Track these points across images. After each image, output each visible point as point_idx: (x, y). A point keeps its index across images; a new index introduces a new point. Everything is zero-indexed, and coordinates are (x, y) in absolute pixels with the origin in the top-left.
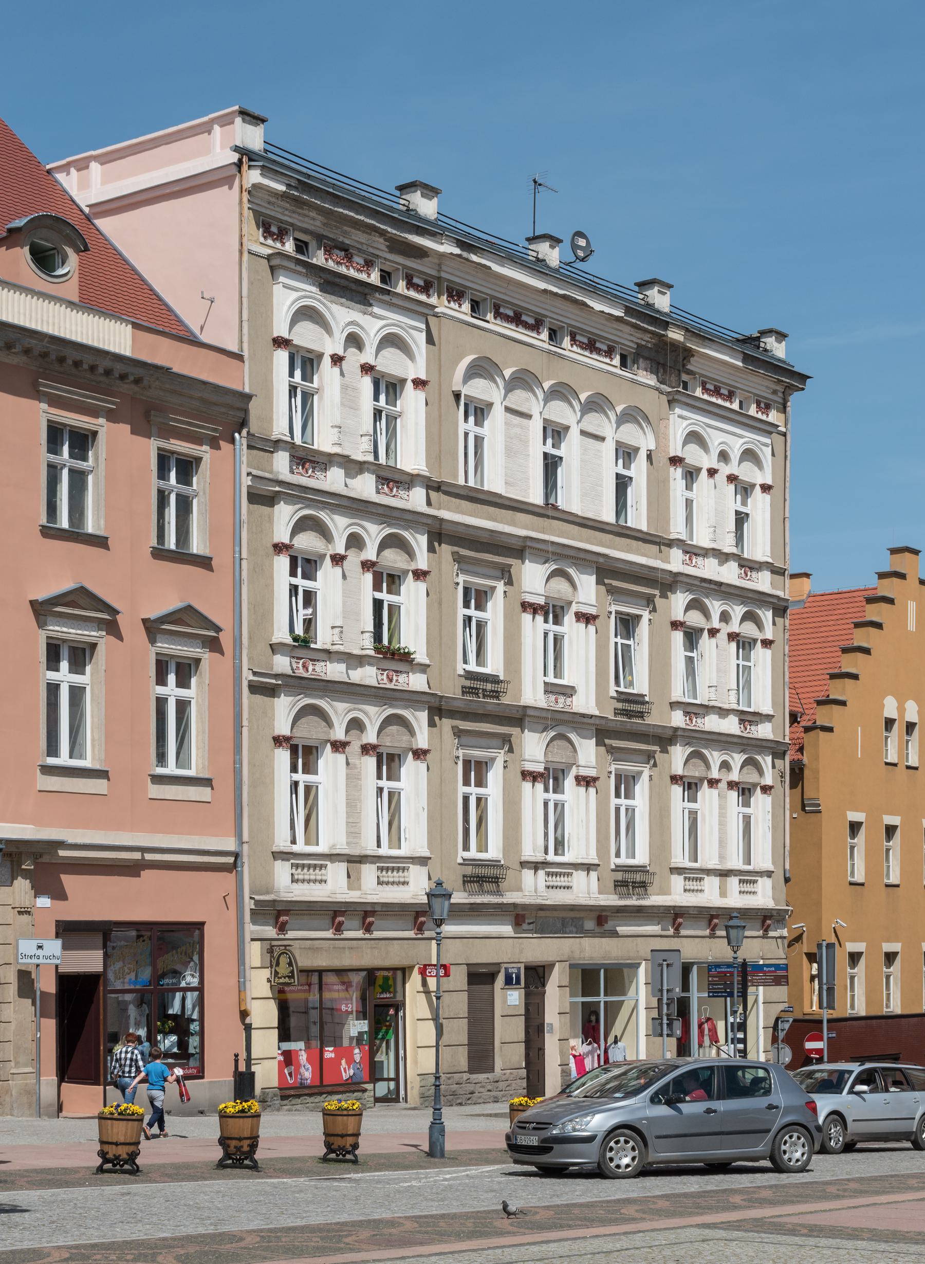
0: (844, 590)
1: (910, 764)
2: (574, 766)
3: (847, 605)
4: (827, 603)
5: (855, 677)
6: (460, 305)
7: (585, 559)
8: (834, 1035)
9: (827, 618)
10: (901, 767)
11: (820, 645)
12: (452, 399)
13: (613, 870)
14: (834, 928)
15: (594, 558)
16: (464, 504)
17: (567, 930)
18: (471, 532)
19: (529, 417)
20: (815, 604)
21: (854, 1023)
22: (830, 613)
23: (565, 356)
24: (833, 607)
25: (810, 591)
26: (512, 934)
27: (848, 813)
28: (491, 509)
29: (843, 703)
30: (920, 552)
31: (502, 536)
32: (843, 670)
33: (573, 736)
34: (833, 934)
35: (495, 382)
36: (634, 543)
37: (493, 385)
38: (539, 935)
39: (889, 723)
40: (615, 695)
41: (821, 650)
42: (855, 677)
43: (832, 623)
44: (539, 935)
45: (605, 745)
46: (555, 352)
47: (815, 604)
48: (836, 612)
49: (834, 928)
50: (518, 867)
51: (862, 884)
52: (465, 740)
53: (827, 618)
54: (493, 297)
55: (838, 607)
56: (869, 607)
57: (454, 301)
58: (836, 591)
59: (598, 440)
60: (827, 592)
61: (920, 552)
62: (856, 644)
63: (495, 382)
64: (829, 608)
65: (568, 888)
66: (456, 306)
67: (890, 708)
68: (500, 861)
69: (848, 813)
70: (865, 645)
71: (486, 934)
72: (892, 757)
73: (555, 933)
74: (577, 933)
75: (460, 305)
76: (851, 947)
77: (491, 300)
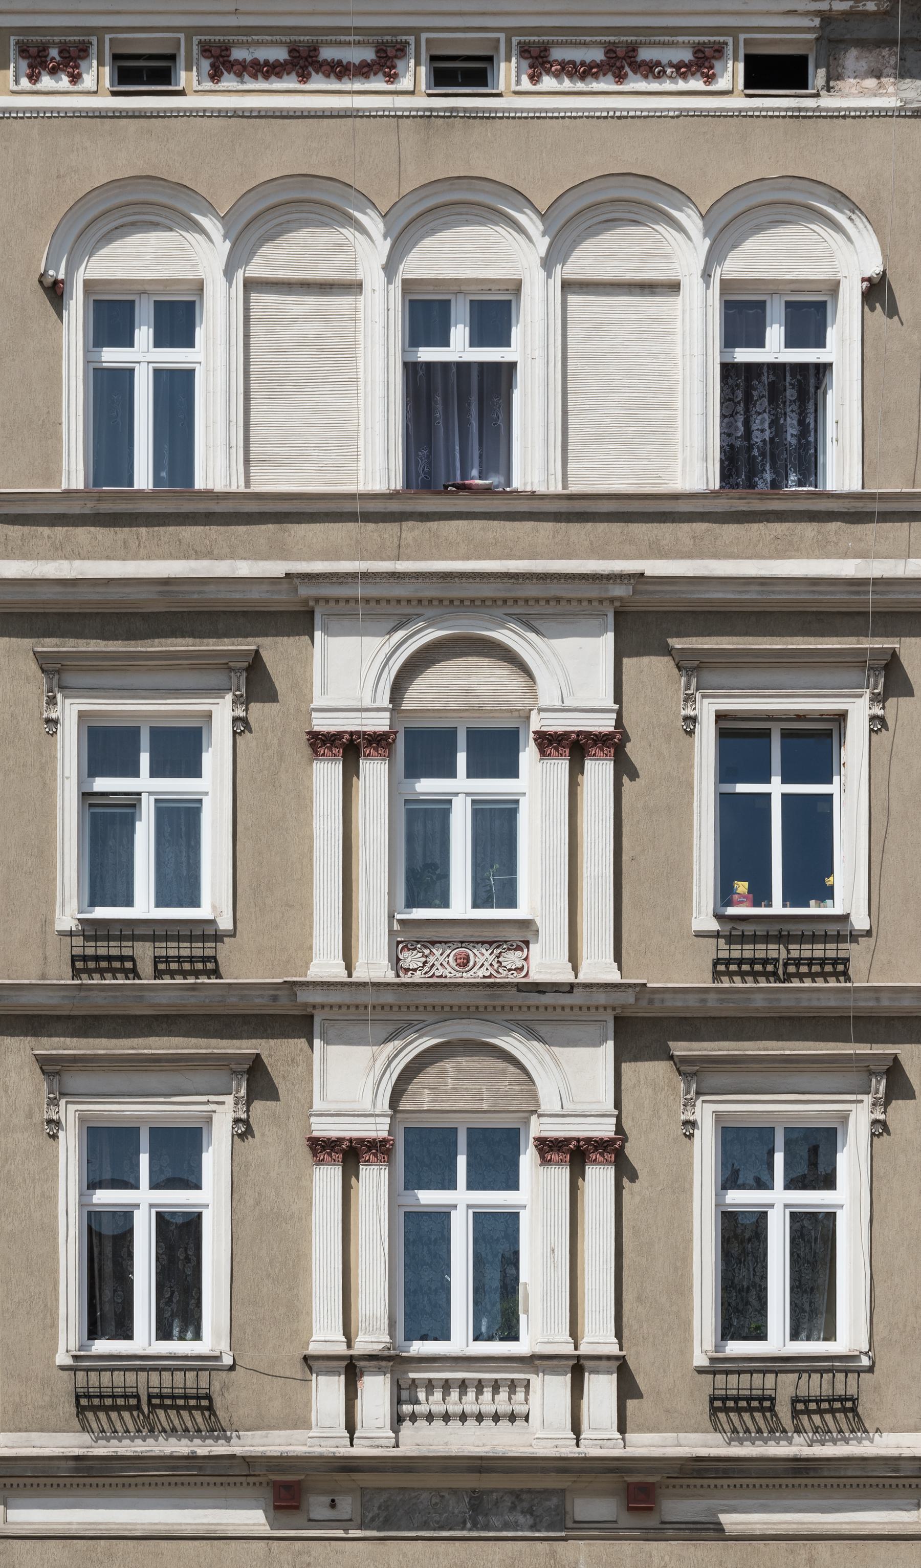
2: (534, 1118)
6: (75, 78)
7: (558, 600)
12: (41, 300)
13: (701, 1371)
15: (593, 591)
16: (82, 533)
17: (495, 1520)
18: (115, 594)
19: (353, 287)
23: (496, 110)
26: (266, 1531)
28: (188, 533)
31: (206, 588)
33: (512, 1043)
35: (202, 230)
36: (808, 530)
37: (194, 238)
38: (375, 1533)
40: (714, 926)
44: (375, 1533)
45: (671, 1058)
46: (452, 109)
50: (298, 1370)
52: (76, 1081)
54: (190, 31)
57: (53, 72)
59: (653, 294)
63: (202, 230)
65: (512, 1417)
66: (64, 82)
68: (217, 1358)
71: (161, 1530)
73: (442, 1528)
74: (533, 1528)
75: (75, 78)
77: (189, 40)
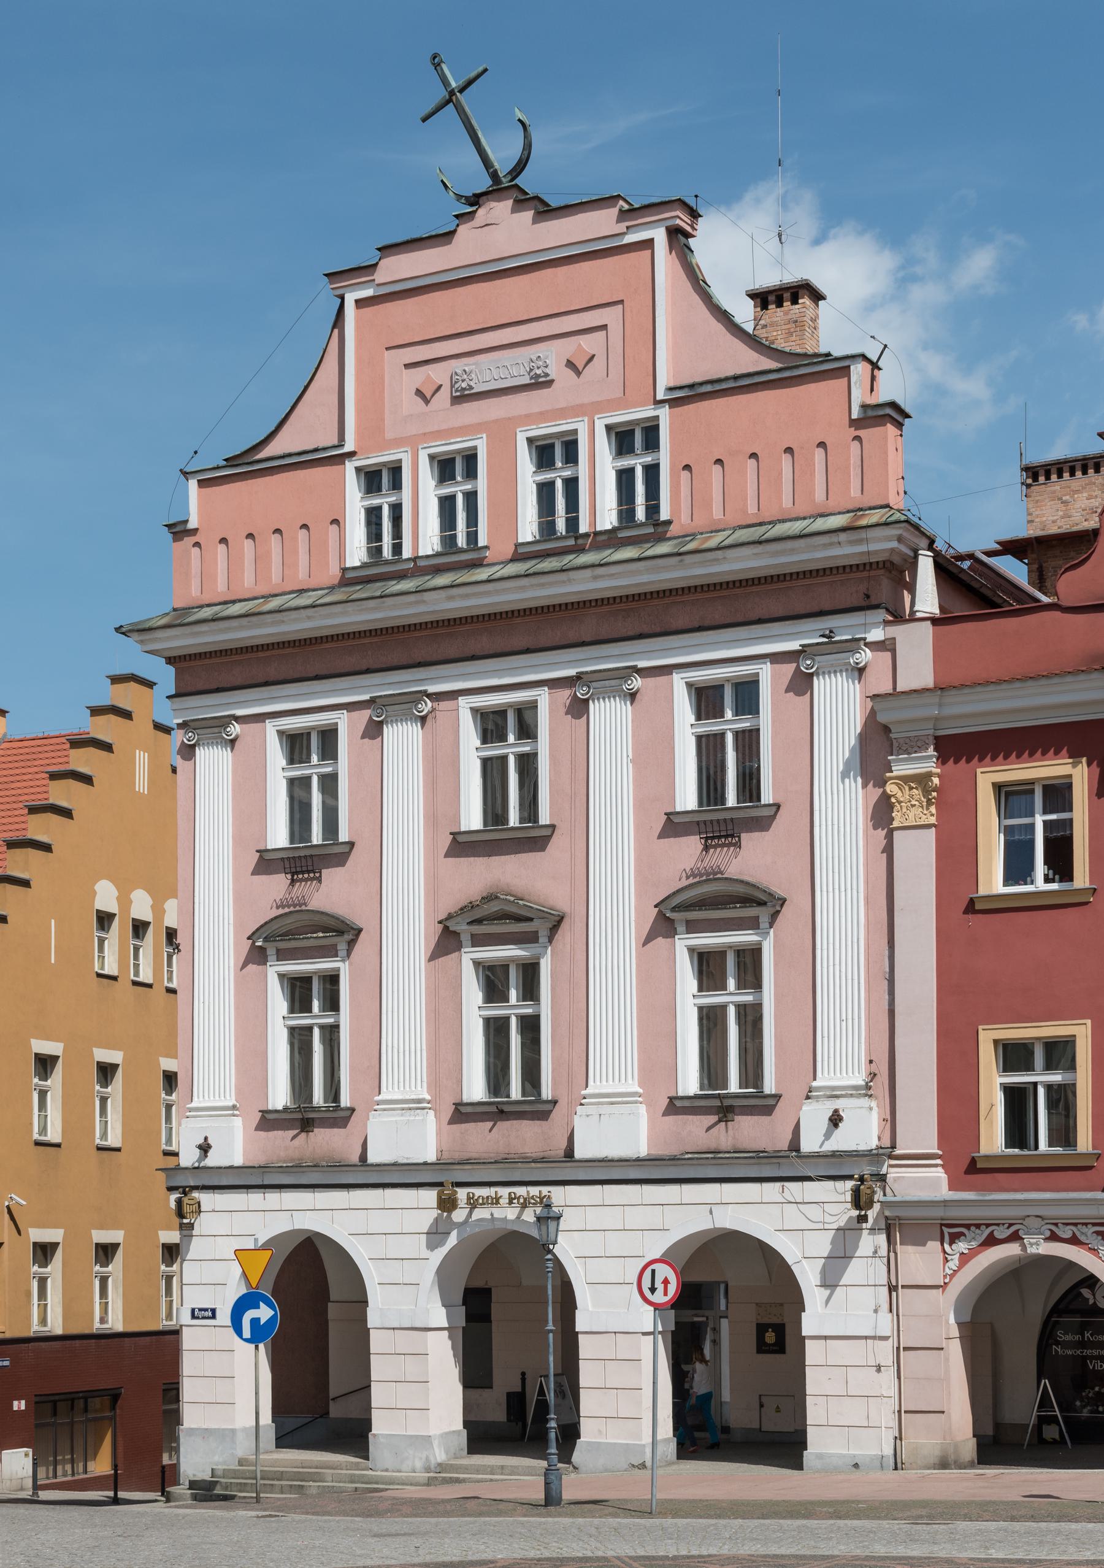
0: (52, 734)
1: (141, 979)
3: (53, 754)
4: (27, 751)
5: (47, 848)
8: (7, 1363)
9: (24, 771)
10: (124, 984)
11: (8, 806)
14: (8, 1207)
20: (9, 752)
21: (43, 1344)
22: (29, 763)
24: (34, 756)
25: (5, 735)
27: (33, 1042)
29: (26, 883)
30: (155, 684)
32: (29, 836)
34: (7, 1216)
39: (104, 920)
41: (9, 813)
42: (47, 848)
43: (30, 777)
47: (9, 752)
48: (36, 763)
49: (8, 1207)
51: (58, 1145)
53: (24, 771)
55: (41, 756)
56: (74, 753)
58: (40, 735)
60: (28, 737)
61: (155, 684)
62: (51, 801)
64: (28, 757)
67: (106, 897)
69: (33, 1042)
70: (64, 804)
72: (111, 967)
76: (38, 1235)
